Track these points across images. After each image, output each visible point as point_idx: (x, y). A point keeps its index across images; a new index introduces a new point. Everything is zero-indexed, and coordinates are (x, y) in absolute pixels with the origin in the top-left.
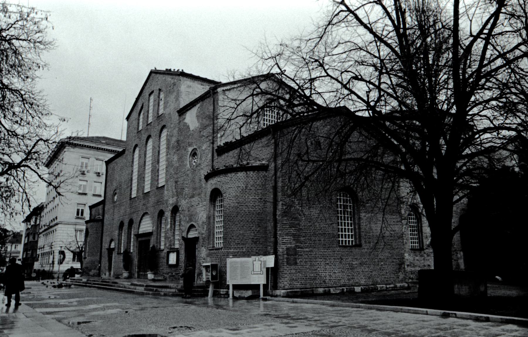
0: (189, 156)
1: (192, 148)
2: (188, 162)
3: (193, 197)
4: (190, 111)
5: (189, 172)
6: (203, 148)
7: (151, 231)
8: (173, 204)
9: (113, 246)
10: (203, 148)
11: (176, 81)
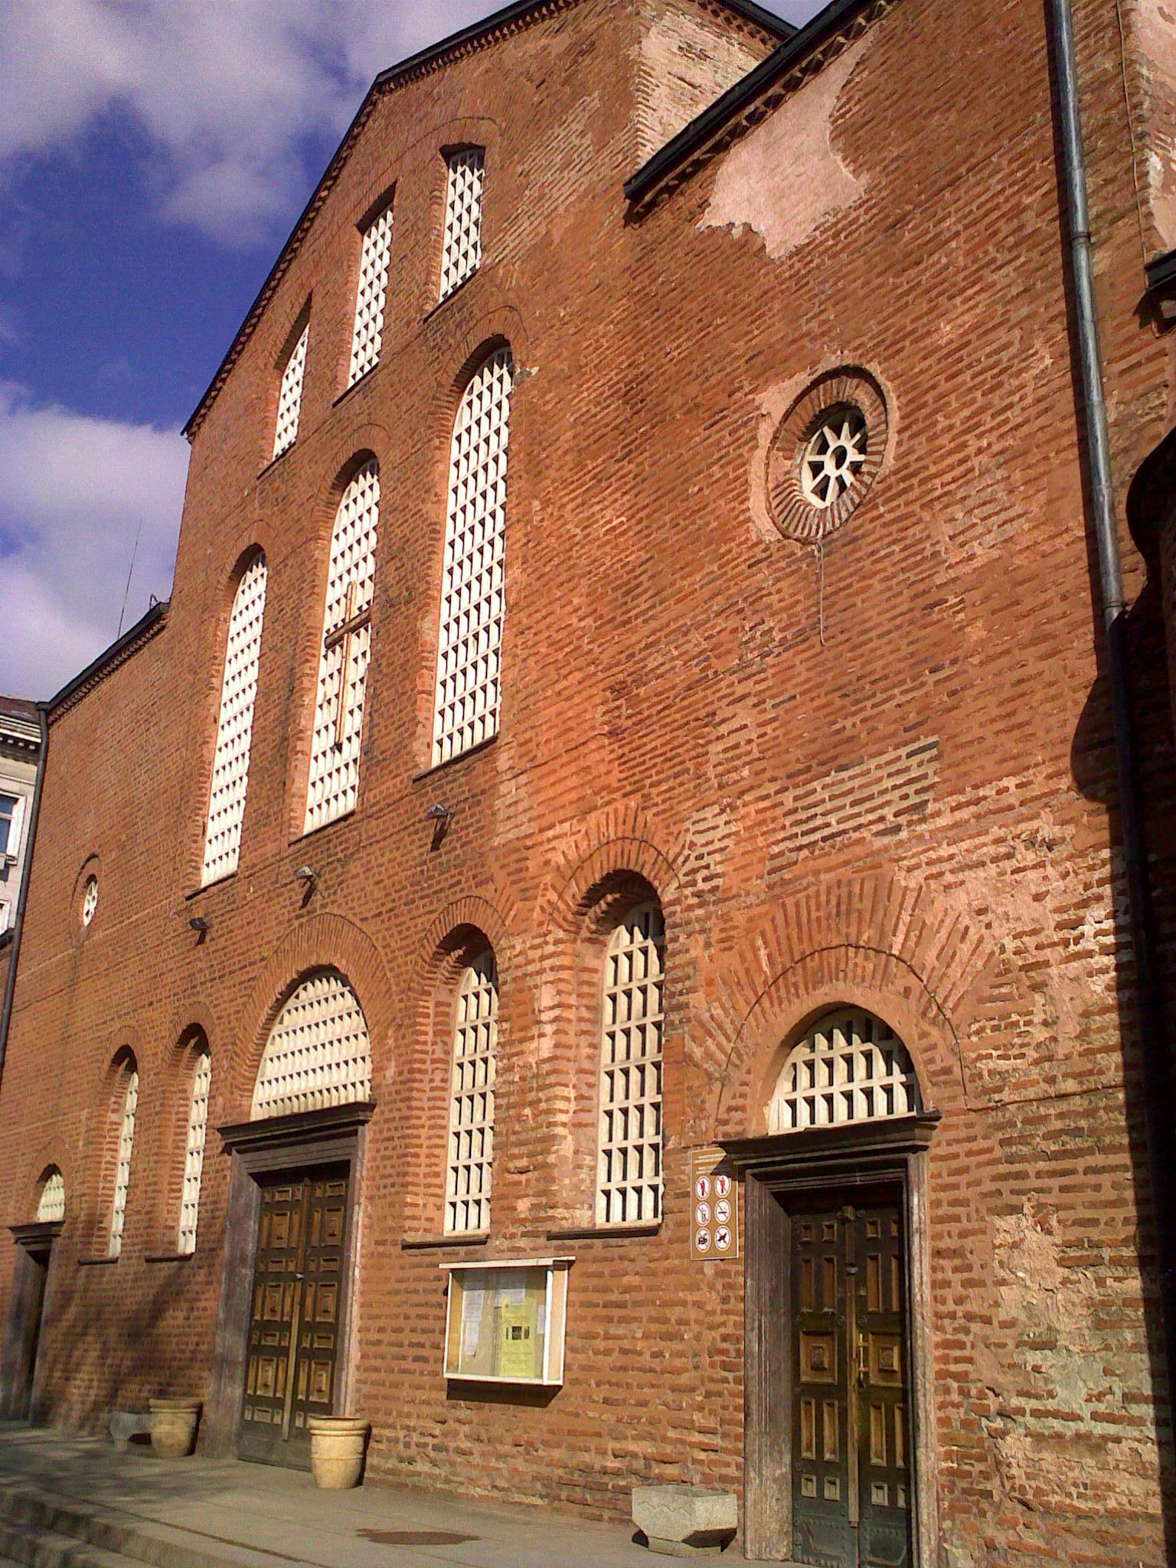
0: (760, 454)
1: (804, 379)
2: (757, 503)
3: (834, 755)
4: (760, 133)
5: (764, 576)
6: (946, 332)
7: (361, 1094)
8: (576, 870)
9: (51, 1206)
10: (946, 332)
11: (589, 26)
